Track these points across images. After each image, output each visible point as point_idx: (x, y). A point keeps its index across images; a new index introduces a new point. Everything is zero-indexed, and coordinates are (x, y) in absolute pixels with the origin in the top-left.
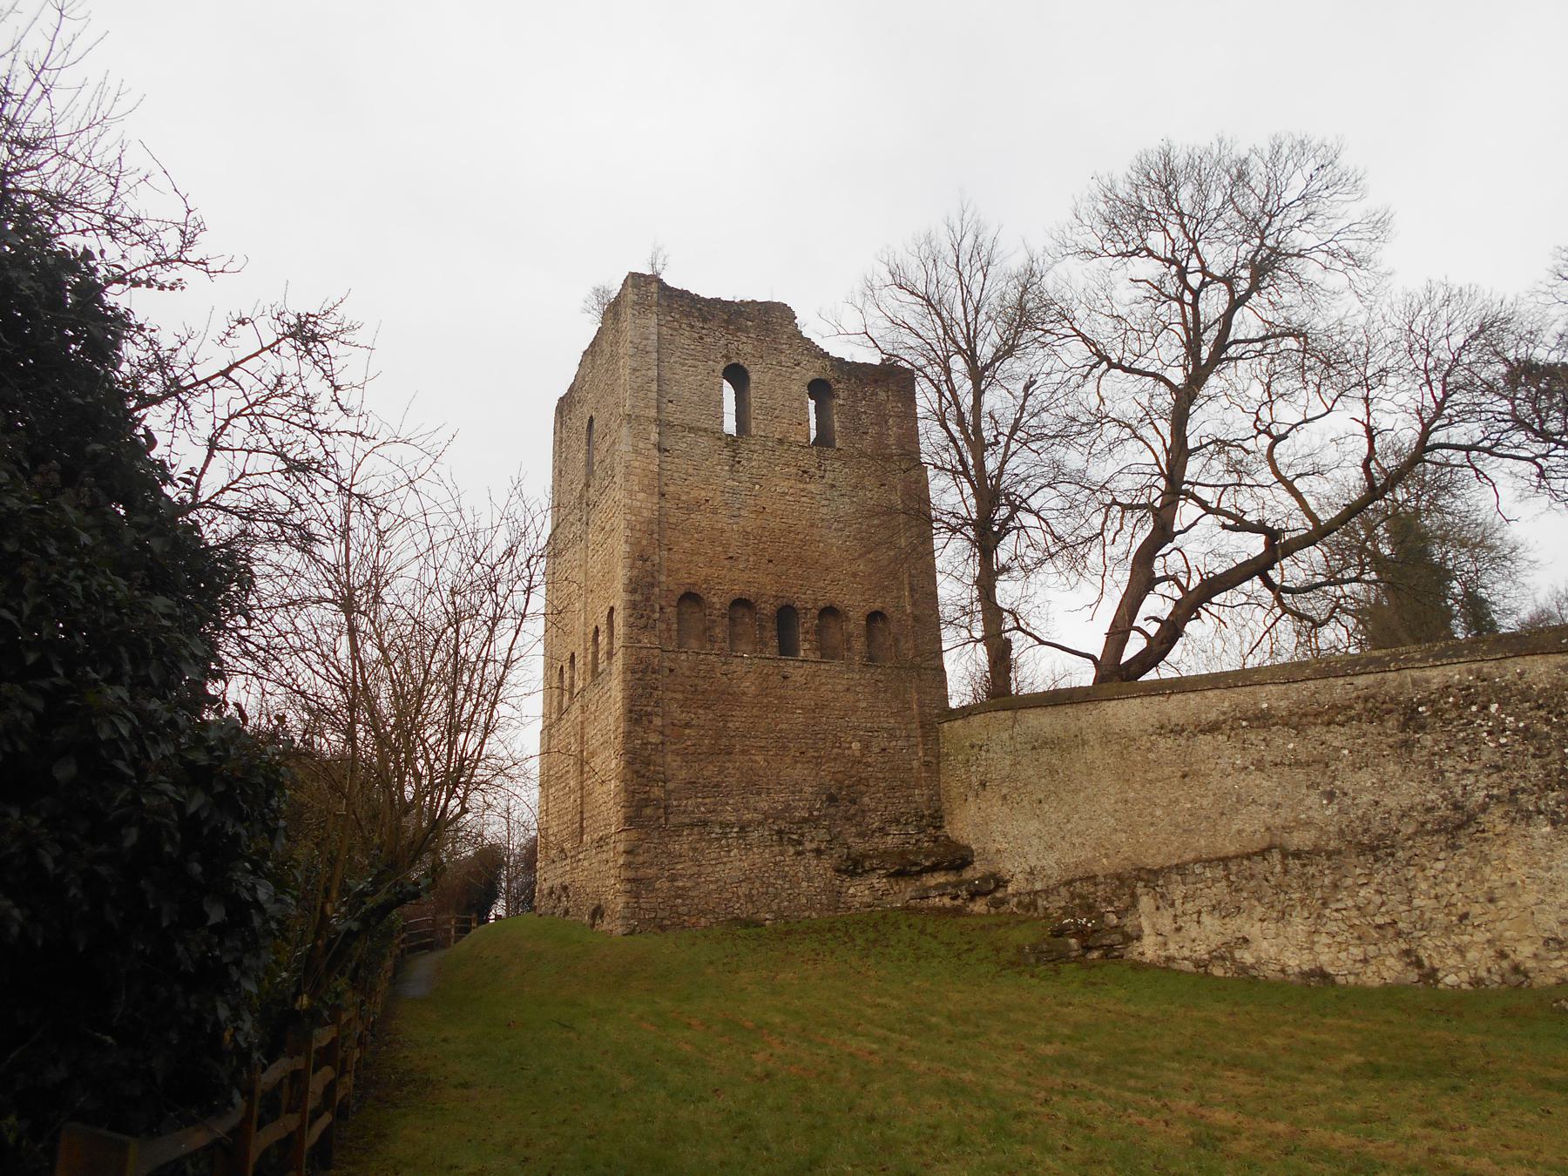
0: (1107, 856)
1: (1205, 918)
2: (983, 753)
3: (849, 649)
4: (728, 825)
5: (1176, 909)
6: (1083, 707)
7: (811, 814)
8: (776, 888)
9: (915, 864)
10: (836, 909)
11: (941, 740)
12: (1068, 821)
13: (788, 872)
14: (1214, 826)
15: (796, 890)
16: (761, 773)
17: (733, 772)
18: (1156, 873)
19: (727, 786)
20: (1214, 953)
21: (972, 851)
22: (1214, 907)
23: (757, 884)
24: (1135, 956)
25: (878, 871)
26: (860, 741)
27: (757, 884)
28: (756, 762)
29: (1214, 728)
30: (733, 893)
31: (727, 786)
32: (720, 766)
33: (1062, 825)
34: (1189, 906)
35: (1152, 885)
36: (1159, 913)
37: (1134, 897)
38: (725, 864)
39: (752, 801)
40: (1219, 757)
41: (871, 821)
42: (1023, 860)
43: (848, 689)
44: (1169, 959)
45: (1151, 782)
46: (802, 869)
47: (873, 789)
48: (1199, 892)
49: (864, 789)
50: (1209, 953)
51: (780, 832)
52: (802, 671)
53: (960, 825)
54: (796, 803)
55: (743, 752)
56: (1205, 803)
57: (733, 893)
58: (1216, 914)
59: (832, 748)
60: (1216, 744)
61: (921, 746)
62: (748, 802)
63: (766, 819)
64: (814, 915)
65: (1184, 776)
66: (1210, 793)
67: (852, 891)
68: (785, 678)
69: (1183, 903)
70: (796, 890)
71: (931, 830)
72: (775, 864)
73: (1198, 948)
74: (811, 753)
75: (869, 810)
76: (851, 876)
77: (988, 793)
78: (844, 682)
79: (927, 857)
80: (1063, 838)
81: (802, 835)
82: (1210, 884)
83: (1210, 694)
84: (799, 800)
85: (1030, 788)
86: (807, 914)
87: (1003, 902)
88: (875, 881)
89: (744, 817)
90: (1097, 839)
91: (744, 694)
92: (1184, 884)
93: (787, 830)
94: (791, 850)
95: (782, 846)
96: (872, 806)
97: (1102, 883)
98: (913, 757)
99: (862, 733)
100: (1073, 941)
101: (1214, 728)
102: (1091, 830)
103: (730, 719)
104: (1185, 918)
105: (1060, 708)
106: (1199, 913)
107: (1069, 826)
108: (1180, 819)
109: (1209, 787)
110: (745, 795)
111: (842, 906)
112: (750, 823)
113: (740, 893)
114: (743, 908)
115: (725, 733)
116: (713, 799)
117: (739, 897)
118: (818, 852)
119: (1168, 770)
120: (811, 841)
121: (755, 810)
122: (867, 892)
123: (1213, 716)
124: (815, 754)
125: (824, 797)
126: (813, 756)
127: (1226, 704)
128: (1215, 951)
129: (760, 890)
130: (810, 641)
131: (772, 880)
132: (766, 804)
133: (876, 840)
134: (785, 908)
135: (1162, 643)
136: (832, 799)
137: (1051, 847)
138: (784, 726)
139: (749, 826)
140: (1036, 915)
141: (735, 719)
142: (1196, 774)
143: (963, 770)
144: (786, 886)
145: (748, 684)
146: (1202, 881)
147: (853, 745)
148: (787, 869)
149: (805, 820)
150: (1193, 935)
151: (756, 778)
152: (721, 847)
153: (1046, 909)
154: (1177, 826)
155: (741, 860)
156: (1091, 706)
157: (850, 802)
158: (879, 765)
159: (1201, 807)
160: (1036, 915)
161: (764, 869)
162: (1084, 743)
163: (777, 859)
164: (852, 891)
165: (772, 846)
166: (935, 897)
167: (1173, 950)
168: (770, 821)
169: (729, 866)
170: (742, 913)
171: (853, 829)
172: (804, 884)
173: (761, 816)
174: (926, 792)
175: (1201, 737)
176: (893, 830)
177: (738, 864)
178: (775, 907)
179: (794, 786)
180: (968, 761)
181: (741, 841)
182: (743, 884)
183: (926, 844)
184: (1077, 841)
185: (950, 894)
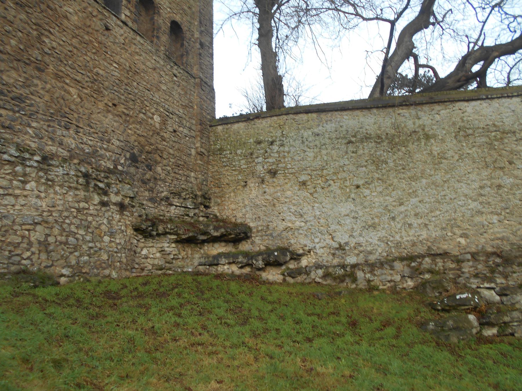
0: (464, 236)
2: (275, 148)
3: (158, 37)
4: (27, 151)
6: (426, 108)
7: (115, 167)
8: (77, 239)
9: (205, 233)
10: (132, 269)
11: (213, 138)
12: (401, 204)
13: (90, 223)
15: (98, 245)
16: (73, 107)
17: (41, 92)
19: (31, 105)
21: (250, 228)
23: (56, 231)
25: (169, 236)
26: (160, 116)
27: (56, 231)
28: (69, 93)
30: (23, 237)
31: (31, 105)
32: (27, 79)
38: (16, 197)
39: (59, 133)
41: (161, 189)
42: (327, 237)
43: (154, 69)
46: (105, 221)
47: (165, 162)
49: (159, 159)
51: (86, 176)
52: (122, 31)
53: (233, 206)
54: (103, 152)
55: (57, 77)
57: (23, 237)
59: (140, 112)
61: (199, 139)
62: (54, 132)
63: (72, 157)
64: (114, 274)
67: (145, 252)
68: (107, 29)
70: (98, 245)
71: (202, 208)
72: (79, 210)
74: (121, 108)
75: (160, 180)
76: (145, 237)
77: (280, 179)
78: (153, 61)
79: (216, 229)
80: (393, 219)
81: (108, 185)
84: (106, 150)
85: (341, 175)
86: (107, 272)
87: (299, 271)
88: (166, 245)
89: (48, 148)
90: (450, 220)
91: (66, 17)
93: (94, 176)
94: (96, 199)
95: (88, 191)
96: (163, 176)
97: (468, 260)
98: (192, 146)
99: (162, 110)
100: (471, 317)
102: (438, 213)
103: (46, 33)
105: (390, 110)
107: (402, 208)
110: (52, 124)
111: (137, 266)
112: (53, 156)
113: (32, 239)
114: (35, 258)
115: (38, 45)
116: (10, 113)
117: (30, 244)
118: (122, 207)
120: (117, 194)
121: (61, 144)
122: (158, 255)
124: (125, 111)
125: (128, 155)
126: (123, 112)
129: (59, 238)
130: (131, 12)
131: (73, 228)
132: (73, 141)
133: (163, 208)
134: (85, 263)
135: (459, 81)
136: (134, 159)
137: (374, 226)
138: (101, 72)
139: (52, 159)
140: (354, 286)
141: (52, 37)
143: (243, 162)
144: (88, 238)
145: (71, 10)
147: (155, 117)
148: (90, 219)
149: (109, 171)
151: (67, 110)
152: (15, 174)
153: (369, 281)
155: (38, 197)
156: (437, 107)
157: (147, 166)
158: (171, 143)
160: (354, 286)
161: (66, 214)
162: (427, 137)
163: (82, 205)
164: (145, 252)
165: (76, 189)
166: (224, 265)
168: (76, 161)
169: (21, 201)
170: (33, 265)
171: (147, 194)
172: (106, 239)
173: (66, 154)
174: (200, 176)
176: (176, 201)
177: (34, 200)
178: (73, 262)
179: (103, 133)
180: (252, 154)
181: (41, 174)
182: (39, 228)
183: (201, 219)
185: (241, 263)
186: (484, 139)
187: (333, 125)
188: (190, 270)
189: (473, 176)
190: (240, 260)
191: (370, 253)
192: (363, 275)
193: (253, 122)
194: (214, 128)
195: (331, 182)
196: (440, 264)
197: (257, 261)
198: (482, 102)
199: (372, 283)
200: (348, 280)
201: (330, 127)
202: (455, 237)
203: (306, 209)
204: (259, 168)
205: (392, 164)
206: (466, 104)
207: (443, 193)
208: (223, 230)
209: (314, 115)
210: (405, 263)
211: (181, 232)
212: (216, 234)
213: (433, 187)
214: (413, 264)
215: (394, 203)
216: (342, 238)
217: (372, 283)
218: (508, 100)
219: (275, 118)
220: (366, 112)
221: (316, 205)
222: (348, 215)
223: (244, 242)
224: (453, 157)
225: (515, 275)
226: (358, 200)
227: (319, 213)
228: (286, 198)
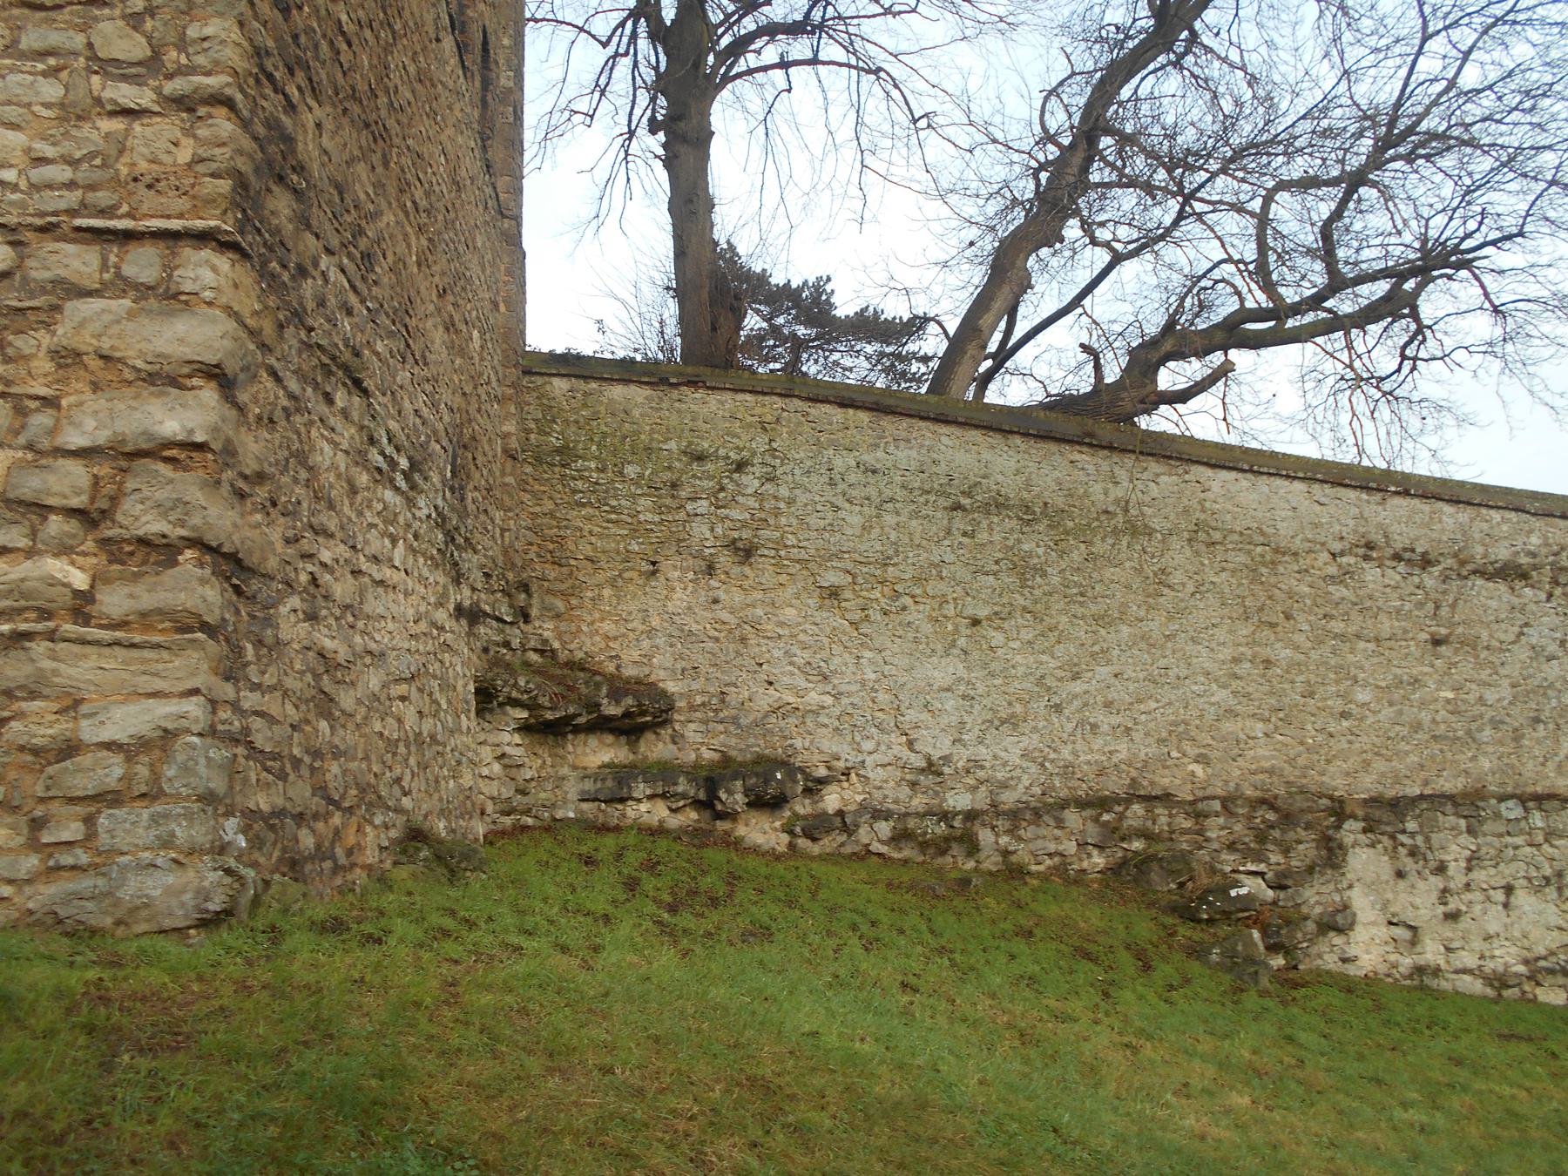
0: (1201, 759)
1: (1522, 898)
2: (750, 482)
5: (1448, 879)
6: (1129, 460)
12: (1076, 677)
14: (1515, 739)
18: (1398, 806)
20: (1542, 963)
22: (1547, 879)
24: (1330, 962)
29: (1511, 573)
33: (1049, 681)
34: (1479, 875)
35: (1389, 829)
36: (1402, 884)
37: (1332, 855)
40: (1526, 625)
42: (896, 739)
44: (1420, 970)
45: (1342, 637)
48: (1510, 852)
50: (1526, 962)
53: (608, 627)
56: (1490, 696)
58: (1551, 892)
60: (1516, 601)
65: (1437, 642)
66: (1505, 683)
69: (1469, 869)
73: (1497, 953)
77: (763, 570)
80: (1058, 708)
82: (1540, 838)
83: (1496, 515)
90: (1175, 724)
92: (1471, 831)
101: (1511, 573)
102: (1153, 705)
104: (1467, 896)
105: (1053, 447)
106: (1509, 890)
107: (1078, 687)
108: (1425, 717)
109: (1502, 671)
119: (1386, 626)
123: (1502, 553)
127: (1535, 540)
128: (1545, 958)
137: (1012, 722)
140: (971, 865)
142: (1470, 644)
146: (1521, 832)
150: (1493, 928)
153: (1006, 853)
154: (1417, 727)
156: (1154, 467)
159: (1481, 700)
160: (971, 865)
166: (639, 801)
167: (1431, 953)
175: (1480, 582)
180: (674, 486)
184: (1106, 721)
186: (1242, 558)
187: (914, 453)
188: (571, 815)
189: (1221, 634)
190: (680, 789)
191: (1004, 786)
192: (993, 839)
193: (675, 394)
194: (539, 380)
195: (907, 601)
196: (1163, 820)
197: (730, 792)
198: (1240, 475)
199: (1014, 859)
200: (956, 849)
201: (906, 456)
202: (1186, 760)
203: (837, 660)
204: (700, 529)
205: (1056, 580)
206: (1209, 472)
207: (1162, 663)
208: (630, 701)
209: (864, 417)
210: (1088, 813)
211: (544, 701)
212: (611, 710)
213: (1143, 645)
214: (1106, 817)
215: (1060, 673)
216: (937, 746)
217: (1014, 859)
218: (1286, 483)
219: (748, 397)
220: (996, 439)
221: (868, 654)
222: (948, 690)
223: (650, 736)
224: (1183, 585)
225: (1301, 847)
226: (976, 655)
227: (873, 676)
228: (781, 624)
